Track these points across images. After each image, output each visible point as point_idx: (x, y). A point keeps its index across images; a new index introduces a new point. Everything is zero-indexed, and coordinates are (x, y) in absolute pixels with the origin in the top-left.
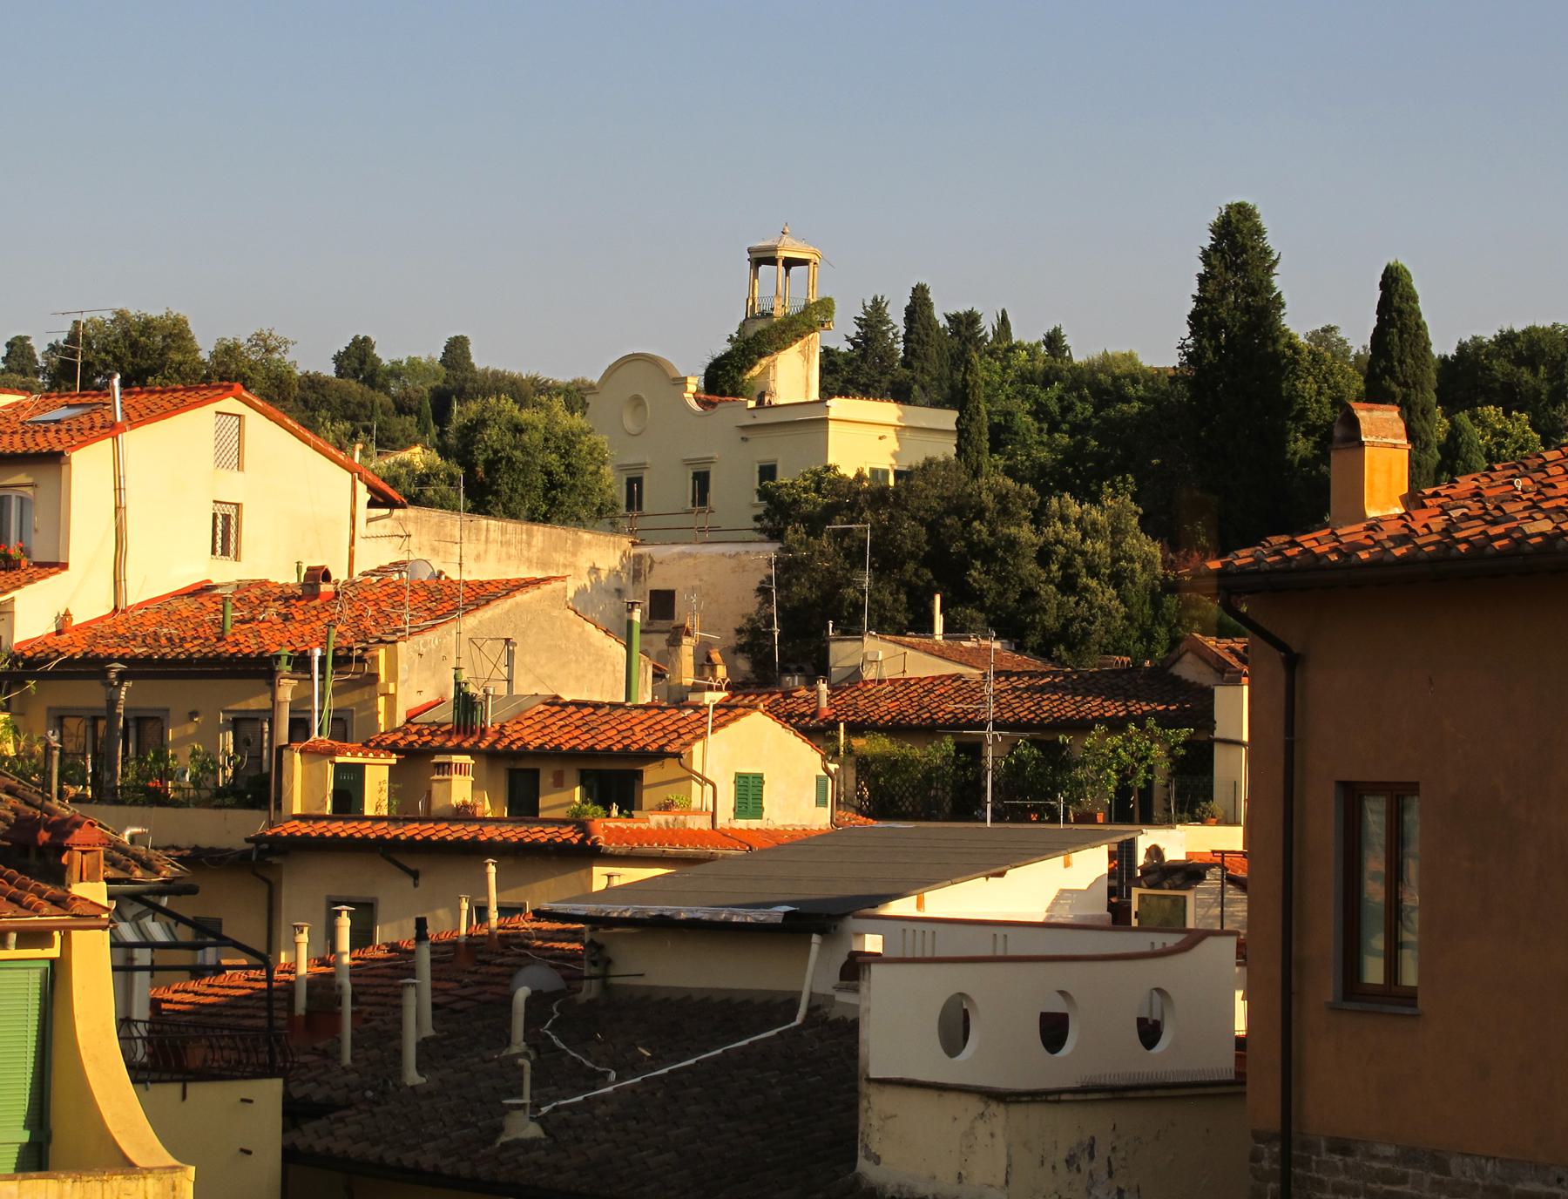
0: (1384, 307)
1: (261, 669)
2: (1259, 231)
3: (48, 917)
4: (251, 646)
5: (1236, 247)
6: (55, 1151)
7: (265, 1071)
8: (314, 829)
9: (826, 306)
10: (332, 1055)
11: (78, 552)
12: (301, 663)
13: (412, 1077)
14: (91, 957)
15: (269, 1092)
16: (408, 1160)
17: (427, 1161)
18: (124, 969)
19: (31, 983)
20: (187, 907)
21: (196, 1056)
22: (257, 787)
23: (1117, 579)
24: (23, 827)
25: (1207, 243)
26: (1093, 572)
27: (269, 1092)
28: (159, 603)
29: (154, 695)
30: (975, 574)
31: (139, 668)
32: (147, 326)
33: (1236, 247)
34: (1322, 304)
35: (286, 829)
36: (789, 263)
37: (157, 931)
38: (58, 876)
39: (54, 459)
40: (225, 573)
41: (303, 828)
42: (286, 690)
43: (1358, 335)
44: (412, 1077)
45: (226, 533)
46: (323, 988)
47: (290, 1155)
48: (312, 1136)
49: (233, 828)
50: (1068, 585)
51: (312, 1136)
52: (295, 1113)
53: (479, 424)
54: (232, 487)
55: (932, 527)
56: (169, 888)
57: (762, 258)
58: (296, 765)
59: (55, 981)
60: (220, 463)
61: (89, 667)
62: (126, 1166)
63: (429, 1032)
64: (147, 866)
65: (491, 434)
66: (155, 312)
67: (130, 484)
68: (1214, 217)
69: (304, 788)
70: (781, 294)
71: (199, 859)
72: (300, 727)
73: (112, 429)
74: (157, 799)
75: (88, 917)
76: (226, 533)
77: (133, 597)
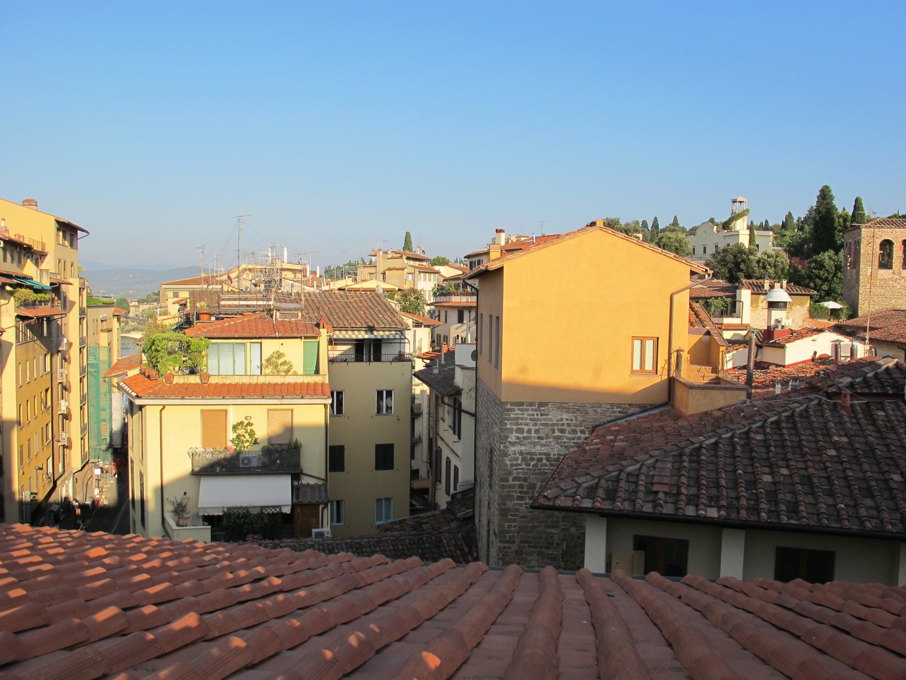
0: (855, 206)
2: (830, 191)
5: (825, 195)
9: (748, 210)
23: (775, 266)
25: (818, 194)
26: (770, 265)
30: (742, 266)
32: (612, 221)
33: (825, 195)
34: (843, 205)
36: (741, 202)
43: (850, 211)
50: (764, 267)
53: (662, 237)
55: (735, 257)
57: (734, 202)
65: (664, 240)
66: (613, 217)
68: (820, 188)
70: (738, 209)
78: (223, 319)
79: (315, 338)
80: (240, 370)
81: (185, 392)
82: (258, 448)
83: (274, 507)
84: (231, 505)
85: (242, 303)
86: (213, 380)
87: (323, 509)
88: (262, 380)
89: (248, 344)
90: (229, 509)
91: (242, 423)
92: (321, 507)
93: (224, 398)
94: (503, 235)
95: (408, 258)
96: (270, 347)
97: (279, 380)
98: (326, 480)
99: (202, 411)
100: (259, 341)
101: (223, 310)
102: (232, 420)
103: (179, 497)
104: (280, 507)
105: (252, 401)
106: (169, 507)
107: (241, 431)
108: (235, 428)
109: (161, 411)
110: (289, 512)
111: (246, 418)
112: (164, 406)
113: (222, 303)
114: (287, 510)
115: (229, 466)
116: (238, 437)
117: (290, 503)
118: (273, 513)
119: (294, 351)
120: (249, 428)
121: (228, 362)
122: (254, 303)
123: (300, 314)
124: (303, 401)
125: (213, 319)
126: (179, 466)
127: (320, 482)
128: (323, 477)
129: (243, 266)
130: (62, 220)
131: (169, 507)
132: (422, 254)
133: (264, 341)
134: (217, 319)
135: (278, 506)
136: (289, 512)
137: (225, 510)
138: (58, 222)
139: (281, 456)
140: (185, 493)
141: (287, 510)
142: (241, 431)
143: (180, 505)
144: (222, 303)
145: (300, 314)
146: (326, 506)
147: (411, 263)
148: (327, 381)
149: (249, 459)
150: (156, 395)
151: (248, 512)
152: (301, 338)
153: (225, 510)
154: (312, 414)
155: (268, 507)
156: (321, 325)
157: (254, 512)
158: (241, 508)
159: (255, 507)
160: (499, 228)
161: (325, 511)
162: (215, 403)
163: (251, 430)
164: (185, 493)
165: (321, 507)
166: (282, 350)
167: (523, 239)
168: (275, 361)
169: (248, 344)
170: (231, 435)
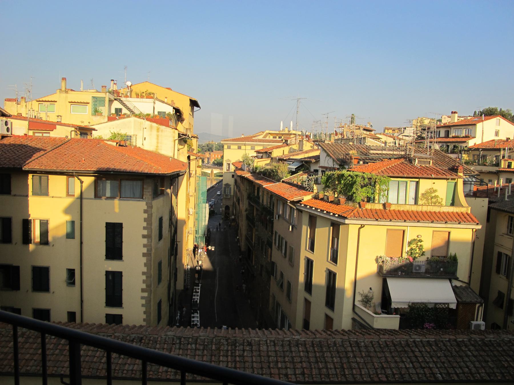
1: (499, 150)
3: (455, 177)
4: (498, 147)
6: (455, 204)
7: (487, 197)
8: (504, 170)
10: (497, 196)
11: (477, 136)
12: (504, 149)
13: (506, 199)
14: (460, 182)
15: (487, 200)
16: (503, 209)
17: (506, 210)
18: (465, 183)
19: (453, 184)
20: (479, 177)
21: (478, 195)
22: (498, 165)
24: (454, 166)
27: (487, 200)
28: (488, 142)
29: (485, 153)
31: (484, 150)
32: (493, 109)
35: (501, 170)
37: (474, 180)
38: (457, 172)
39: (475, 125)
40: (496, 138)
41: (503, 169)
42: (502, 152)
44: (506, 199)
45: (497, 134)
46: (497, 188)
47: (489, 209)
48: (492, 205)
49: (494, 169)
51: (492, 205)
52: (490, 202)
54: (498, 128)
56: (477, 175)
58: (503, 162)
59: (456, 184)
60: (496, 125)
61: (478, 149)
62: (462, 206)
63: (510, 194)
64: (474, 172)
67: (484, 128)
69: (503, 165)
71: (481, 172)
72: (503, 157)
73: (482, 121)
74: (485, 165)
75: (460, 177)
76: (497, 134)
77: (484, 141)
78: (367, 163)
79: (454, 179)
80: (402, 201)
81: (377, 216)
82: (423, 259)
83: (444, 304)
84: (413, 301)
85: (384, 152)
86: (393, 208)
87: (479, 307)
88: (414, 208)
89: (409, 182)
90: (413, 303)
91: (415, 240)
92: (477, 305)
93: (405, 221)
94: (456, 115)
95: (364, 129)
96: (425, 185)
97: (436, 209)
98: (469, 283)
99: (388, 230)
100: (417, 180)
101: (371, 156)
102: (408, 238)
103: (366, 291)
104: (448, 304)
105: (427, 225)
106: (358, 298)
107: (413, 246)
108: (410, 243)
109: (360, 229)
110: (454, 308)
111: (417, 236)
112: (362, 226)
113: (372, 152)
114: (453, 306)
115: (406, 271)
116: (412, 249)
117: (456, 302)
118: (443, 308)
119: (441, 188)
120: (419, 243)
121: (397, 194)
122: (391, 152)
123: (431, 162)
124: (459, 226)
125: (361, 162)
126: (368, 268)
127: (464, 285)
128: (466, 280)
129: (267, 132)
130: (193, 99)
131: (358, 298)
132: (370, 128)
133: (421, 180)
134: (364, 163)
135: (446, 303)
136: (454, 308)
137: (410, 304)
138: (191, 100)
139: (441, 266)
140: (371, 288)
141: (453, 306)
142: (413, 246)
143: (366, 296)
144: (372, 152)
145: (431, 162)
146: (481, 305)
147: (365, 132)
148: (469, 212)
149: (419, 266)
150: (358, 217)
151: (427, 306)
152: (447, 179)
153: (410, 304)
154: (464, 234)
155: (440, 304)
156: (459, 170)
157: (430, 306)
158: (417, 303)
159: (431, 303)
160: (454, 111)
161: (480, 308)
162: (399, 225)
163: (421, 246)
164: (371, 288)
165: (477, 305)
166: (435, 187)
167: (469, 118)
168: (430, 195)
169: (409, 182)
170: (406, 248)
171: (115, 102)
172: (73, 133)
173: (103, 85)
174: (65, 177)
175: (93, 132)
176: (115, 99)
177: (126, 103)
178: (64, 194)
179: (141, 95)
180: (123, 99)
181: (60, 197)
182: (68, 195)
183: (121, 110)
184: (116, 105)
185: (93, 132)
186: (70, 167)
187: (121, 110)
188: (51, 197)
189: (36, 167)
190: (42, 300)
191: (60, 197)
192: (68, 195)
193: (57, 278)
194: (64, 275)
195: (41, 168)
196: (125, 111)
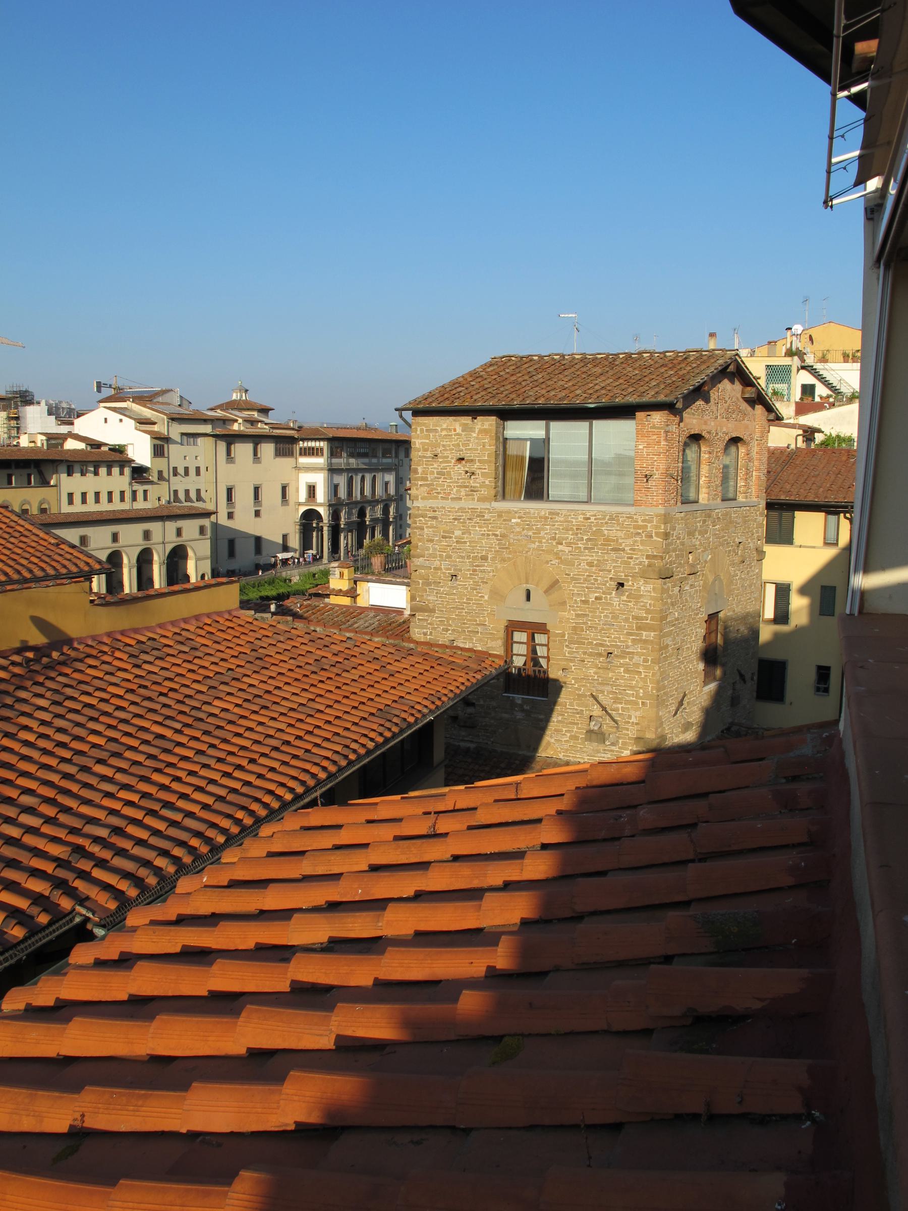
171: (802, 372)
172: (800, 439)
173: (771, 340)
174: (821, 515)
175: (816, 435)
176: (803, 368)
177: (825, 373)
178: (820, 542)
179: (854, 356)
180: (818, 366)
181: (814, 547)
182: (827, 544)
183: (812, 387)
184: (806, 378)
185: (816, 435)
186: (832, 499)
187: (812, 387)
188: (797, 546)
189: (782, 498)
190: (773, 716)
191: (814, 547)
192: (827, 544)
193: (800, 680)
194: (812, 676)
195: (792, 498)
196: (821, 391)
